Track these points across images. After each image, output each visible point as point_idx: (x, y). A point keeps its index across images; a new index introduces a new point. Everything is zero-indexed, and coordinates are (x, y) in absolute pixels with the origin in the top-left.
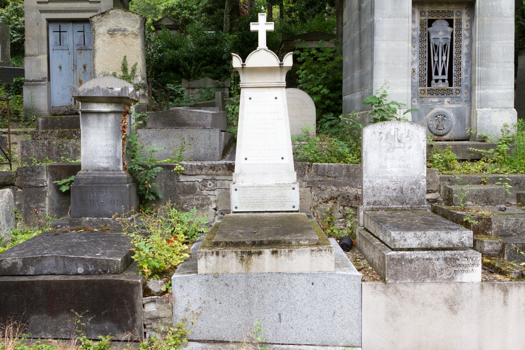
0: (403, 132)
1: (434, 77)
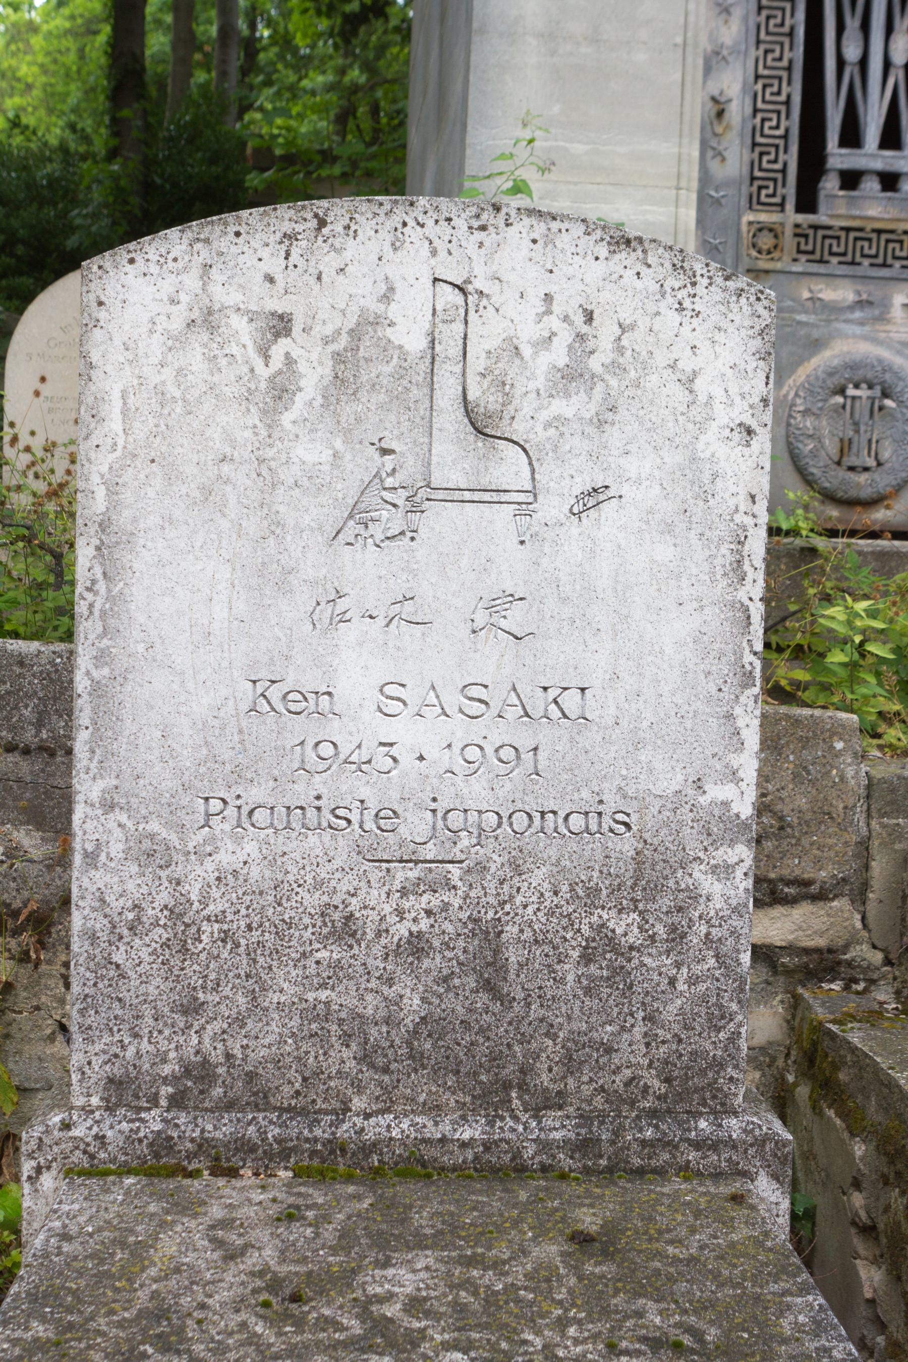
0: (528, 331)
1: (838, 157)
